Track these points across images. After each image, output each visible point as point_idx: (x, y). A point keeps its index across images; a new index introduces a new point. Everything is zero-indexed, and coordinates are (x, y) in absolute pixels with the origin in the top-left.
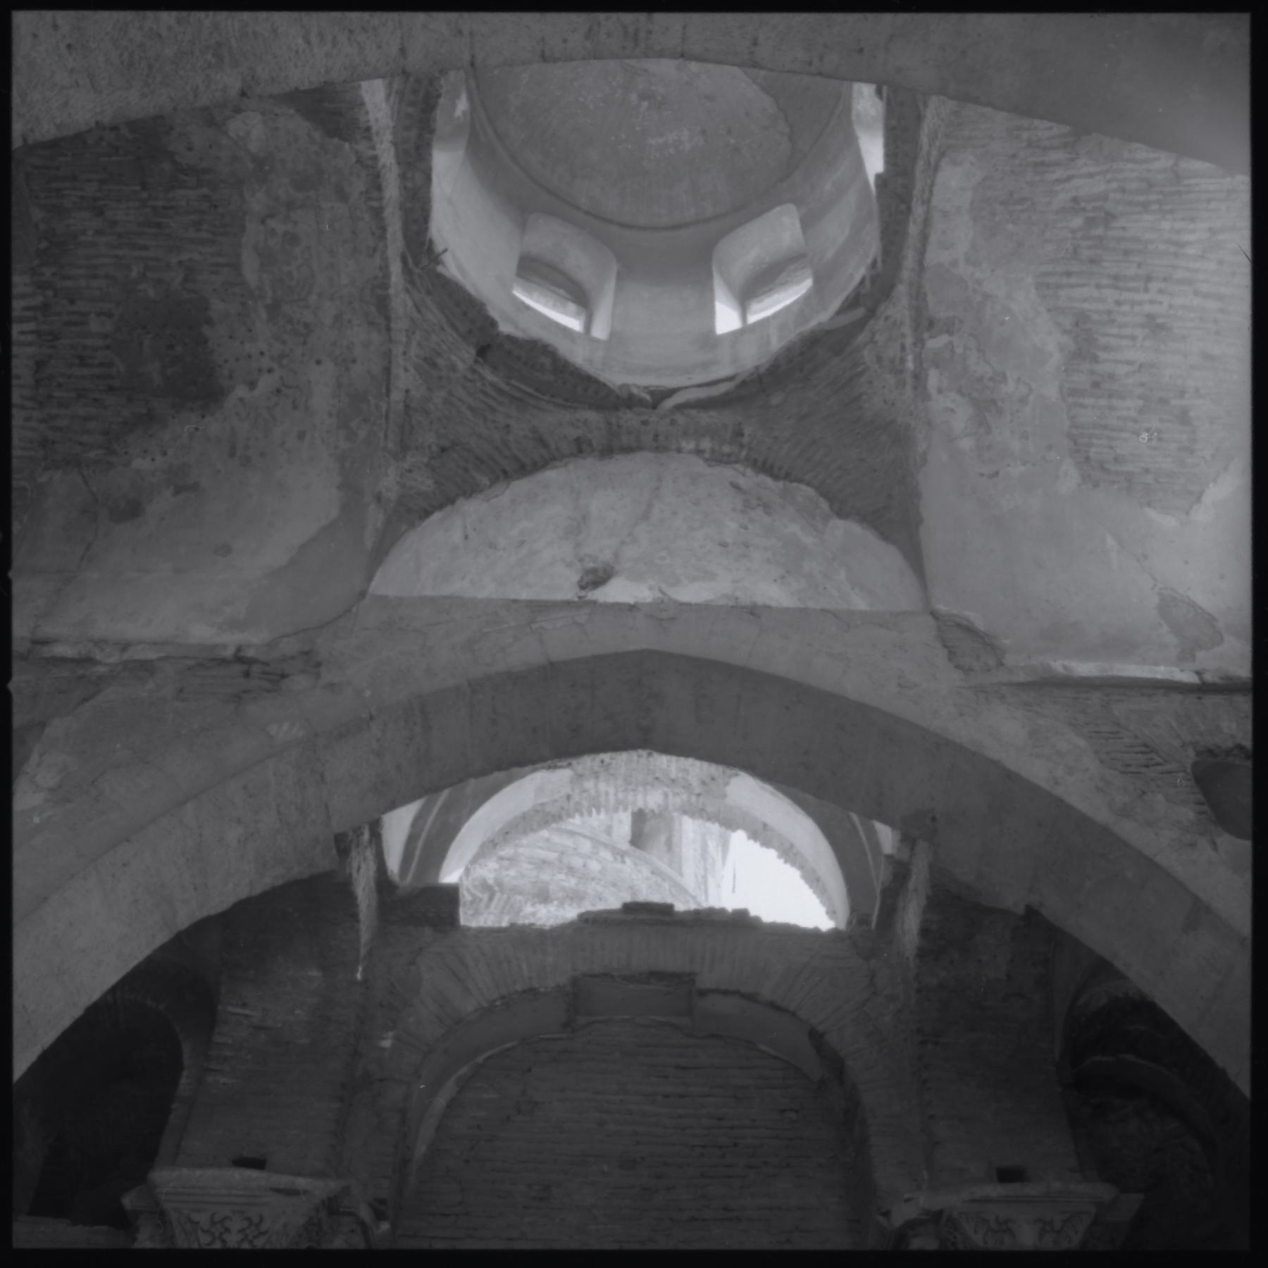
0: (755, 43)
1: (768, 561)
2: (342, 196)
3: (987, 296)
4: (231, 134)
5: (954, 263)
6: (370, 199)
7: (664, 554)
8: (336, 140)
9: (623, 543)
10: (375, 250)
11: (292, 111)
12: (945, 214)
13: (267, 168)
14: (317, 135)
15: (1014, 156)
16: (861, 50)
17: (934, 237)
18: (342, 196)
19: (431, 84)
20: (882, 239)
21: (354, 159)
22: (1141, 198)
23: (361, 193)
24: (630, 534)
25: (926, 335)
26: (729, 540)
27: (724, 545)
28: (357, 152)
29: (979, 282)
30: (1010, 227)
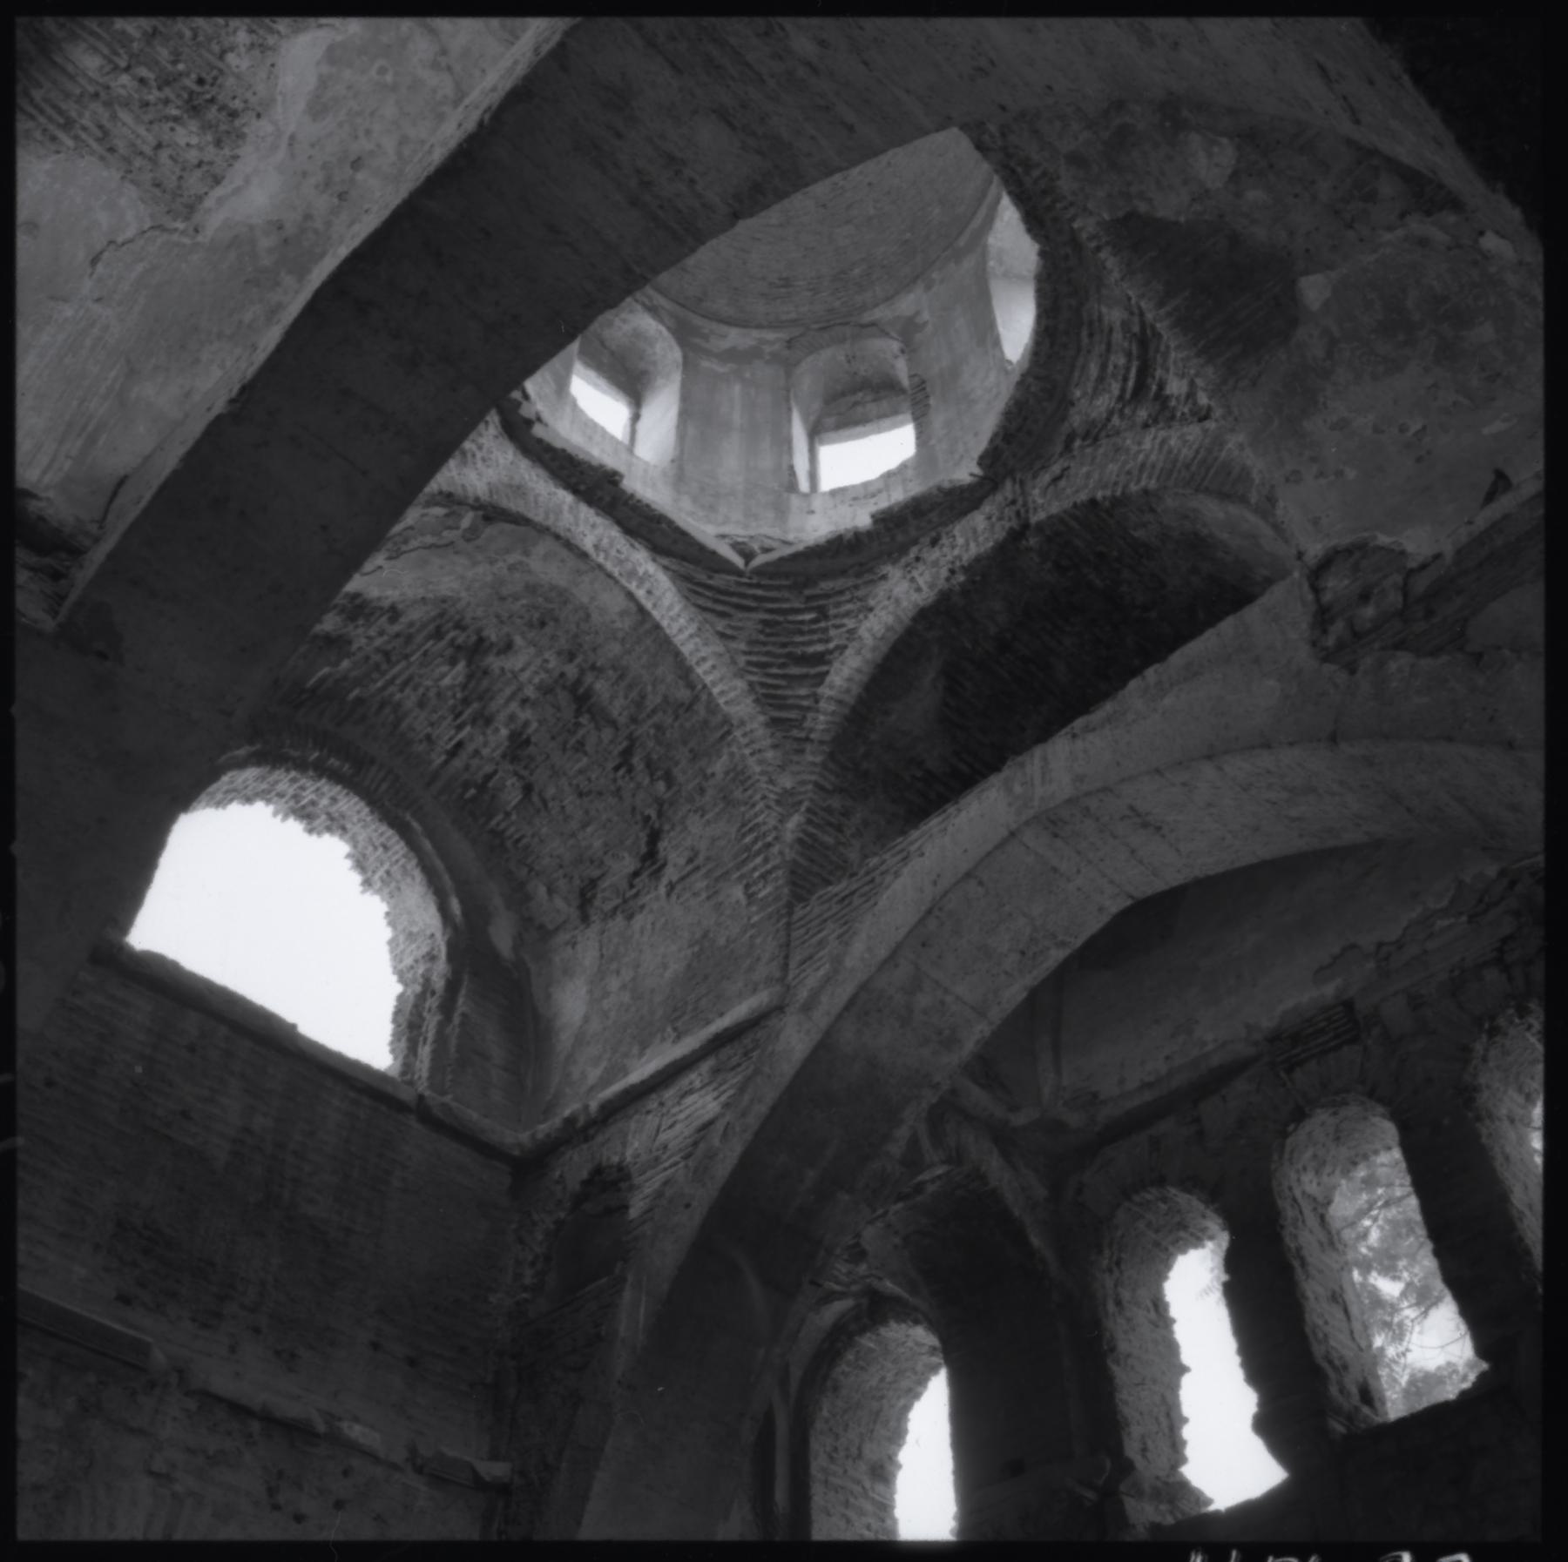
0: (981, 883)
1: (308, 217)
2: (1077, 160)
3: (475, 564)
4: (1225, 141)
5: (526, 553)
6: (1044, 174)
7: (389, 78)
8: (1121, 214)
9: (444, 52)
10: (1003, 135)
11: (1182, 219)
12: (579, 572)
13: (1168, 124)
14: (1143, 207)
15: (594, 650)
16: (924, 945)
17: (564, 553)
18: (1076, 160)
19: (1047, 237)
20: (564, 451)
21: (1090, 206)
22: (471, 686)
23: (1059, 178)
24: (449, 68)
25: (481, 513)
26: (360, 176)
27: (357, 164)
28: (1091, 213)
29: (492, 562)
30: (524, 602)
